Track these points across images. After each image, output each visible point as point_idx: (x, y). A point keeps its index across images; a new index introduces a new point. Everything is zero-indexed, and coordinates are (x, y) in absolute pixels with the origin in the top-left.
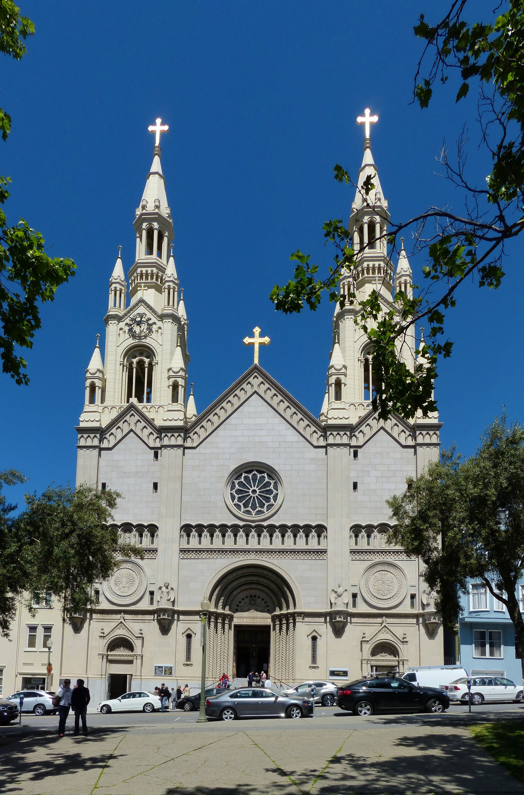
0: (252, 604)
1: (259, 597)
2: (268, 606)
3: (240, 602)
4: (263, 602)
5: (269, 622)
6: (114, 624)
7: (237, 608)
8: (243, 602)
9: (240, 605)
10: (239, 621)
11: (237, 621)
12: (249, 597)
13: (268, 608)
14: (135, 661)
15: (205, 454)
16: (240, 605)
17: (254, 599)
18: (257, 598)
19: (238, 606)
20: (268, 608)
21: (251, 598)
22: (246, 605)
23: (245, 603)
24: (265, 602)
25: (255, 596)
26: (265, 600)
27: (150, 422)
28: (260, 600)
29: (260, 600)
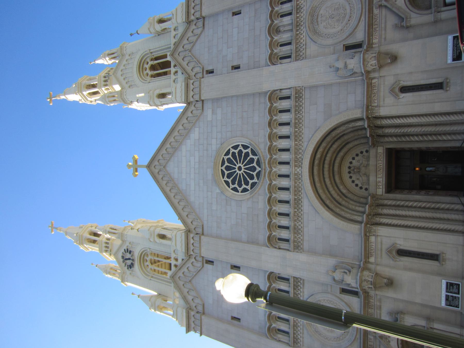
0: (359, 172)
1: (351, 163)
2: (362, 153)
3: (357, 185)
4: (357, 158)
5: (381, 150)
7: (364, 188)
8: (357, 182)
9: (360, 185)
10: (381, 187)
11: (381, 190)
12: (351, 175)
13: (364, 152)
15: (208, 215)
16: (360, 185)
18: (351, 165)
19: (361, 188)
20: (364, 152)
21: (352, 172)
22: (361, 178)
23: (358, 179)
24: (357, 155)
25: (349, 168)
26: (354, 156)
27: (185, 262)
28: (354, 162)
29: (354, 162)
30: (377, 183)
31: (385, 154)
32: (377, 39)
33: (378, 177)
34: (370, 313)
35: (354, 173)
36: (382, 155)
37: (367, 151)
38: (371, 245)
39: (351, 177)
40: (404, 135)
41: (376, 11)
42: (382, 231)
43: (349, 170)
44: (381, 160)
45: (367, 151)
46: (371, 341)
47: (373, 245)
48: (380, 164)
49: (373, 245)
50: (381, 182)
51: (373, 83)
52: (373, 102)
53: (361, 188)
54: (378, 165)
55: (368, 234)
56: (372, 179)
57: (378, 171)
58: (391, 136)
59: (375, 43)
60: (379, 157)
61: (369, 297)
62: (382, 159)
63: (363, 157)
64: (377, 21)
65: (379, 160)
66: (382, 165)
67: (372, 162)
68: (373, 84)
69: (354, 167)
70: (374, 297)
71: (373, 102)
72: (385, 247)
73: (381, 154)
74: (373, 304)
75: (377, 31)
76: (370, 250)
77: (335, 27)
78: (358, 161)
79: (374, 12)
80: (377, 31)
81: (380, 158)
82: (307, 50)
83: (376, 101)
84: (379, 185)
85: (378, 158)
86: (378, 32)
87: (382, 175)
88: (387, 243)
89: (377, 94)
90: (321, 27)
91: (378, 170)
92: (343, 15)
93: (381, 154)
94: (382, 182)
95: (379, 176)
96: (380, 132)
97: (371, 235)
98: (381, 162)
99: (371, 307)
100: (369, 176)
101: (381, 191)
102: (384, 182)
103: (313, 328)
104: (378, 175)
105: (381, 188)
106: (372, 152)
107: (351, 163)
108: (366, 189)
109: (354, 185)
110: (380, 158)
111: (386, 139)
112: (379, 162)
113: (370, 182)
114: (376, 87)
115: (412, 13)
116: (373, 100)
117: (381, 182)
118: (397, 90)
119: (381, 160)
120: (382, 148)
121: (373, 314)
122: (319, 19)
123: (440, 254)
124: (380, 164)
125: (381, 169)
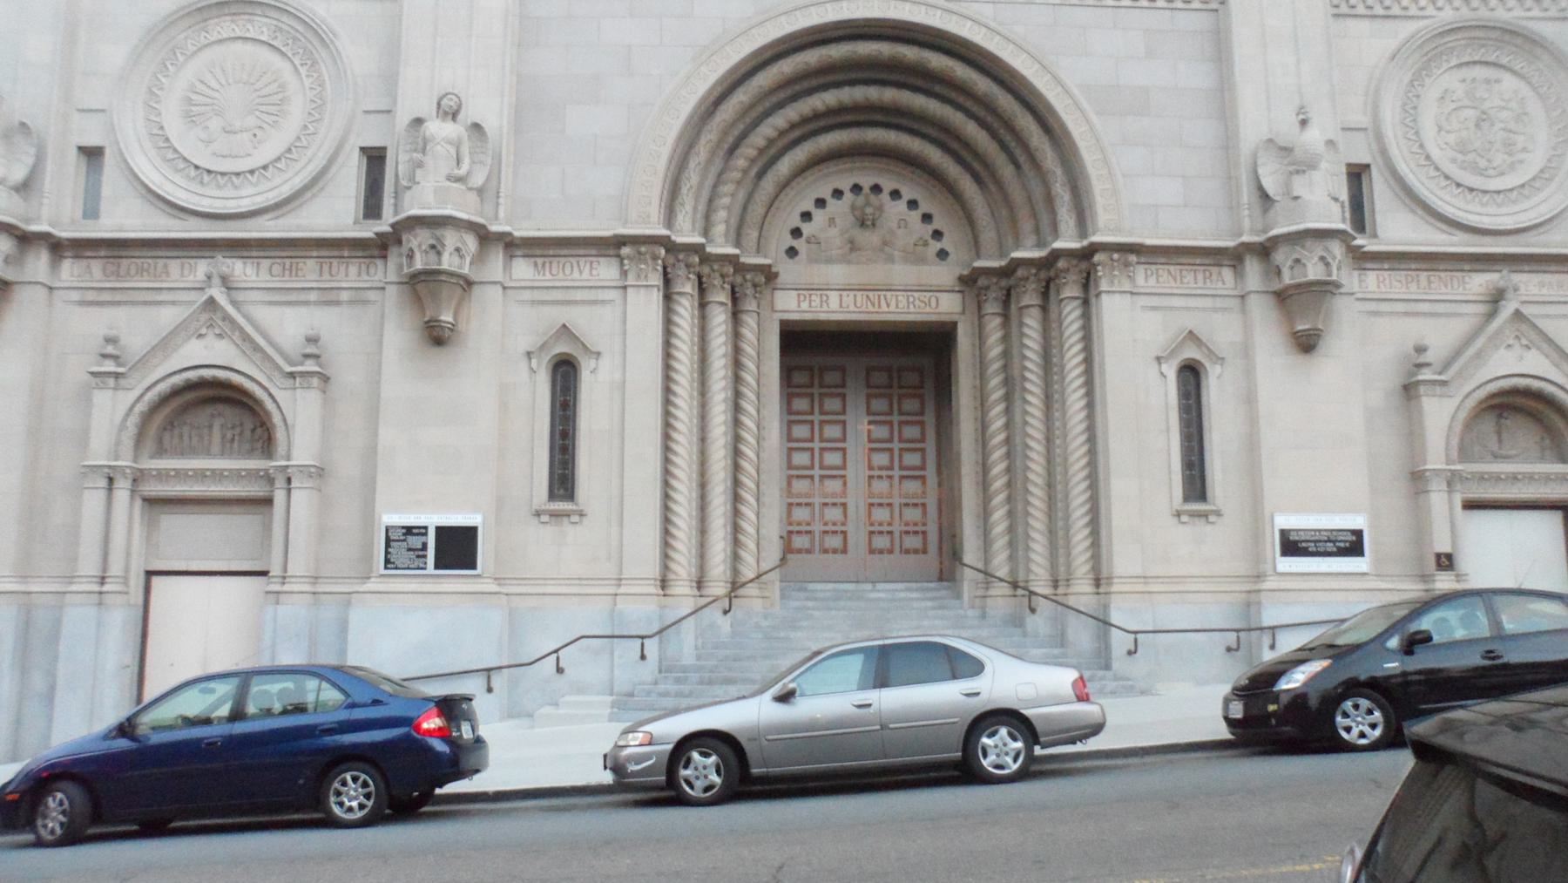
1: (895, 194)
2: (937, 235)
5: (947, 306)
6: (168, 317)
7: (796, 243)
8: (819, 216)
9: (807, 229)
10: (805, 306)
12: (848, 196)
14: (279, 497)
16: (807, 229)
17: (873, 198)
18: (885, 196)
19: (796, 233)
21: (860, 200)
22: (834, 232)
23: (832, 221)
24: (927, 218)
28: (901, 206)
29: (901, 206)
30: (819, 292)
31: (934, 318)
32: (1379, 287)
33: (845, 293)
34: (301, 265)
36: (928, 309)
38: (582, 264)
39: (838, 193)
41: (1480, 282)
42: (645, 305)
43: (866, 189)
44: (911, 306)
45: (942, 254)
46: (186, 272)
47: (581, 272)
48: (893, 303)
49: (581, 272)
50: (825, 304)
51: (1220, 273)
52: (1149, 272)
54: (889, 294)
55: (626, 251)
56: (837, 273)
57: (867, 296)
59: (1363, 277)
60: (922, 298)
61: (367, 261)
62: (912, 309)
63: (921, 243)
64: (1443, 287)
65: (911, 299)
66: (892, 308)
67: (902, 273)
68: (1215, 270)
69: (880, 208)
70: (368, 278)
71: (1149, 272)
72: (579, 319)
73: (933, 304)
74: (338, 278)
75: (1408, 288)
76: (563, 260)
77: (1443, 133)
78: (903, 223)
79: (1474, 275)
80: (1408, 288)
81: (917, 302)
82: (1365, 25)
83: (1152, 281)
84: (813, 297)
85: (916, 294)
86: (1404, 290)
87: (852, 308)
88: (595, 325)
89: (1178, 284)
90: (1448, 80)
91: (871, 294)
92: (1483, 163)
93: (933, 304)
94: (825, 308)
95: (848, 298)
97: (626, 262)
98: (901, 305)
99: (326, 268)
100: (849, 262)
101: (792, 305)
102: (823, 317)
103: (186, 38)
104: (852, 294)
105: (799, 306)
108: (792, 252)
109: (808, 205)
110: (917, 302)
112: (900, 298)
113: (823, 266)
114: (1205, 283)
115: (1456, 401)
116: (1157, 270)
117: (825, 304)
118: (1191, 353)
119: (911, 306)
120: (958, 309)
121: (297, 275)
122: (1480, 72)
123: (577, 504)
124: (893, 303)
125: (873, 305)
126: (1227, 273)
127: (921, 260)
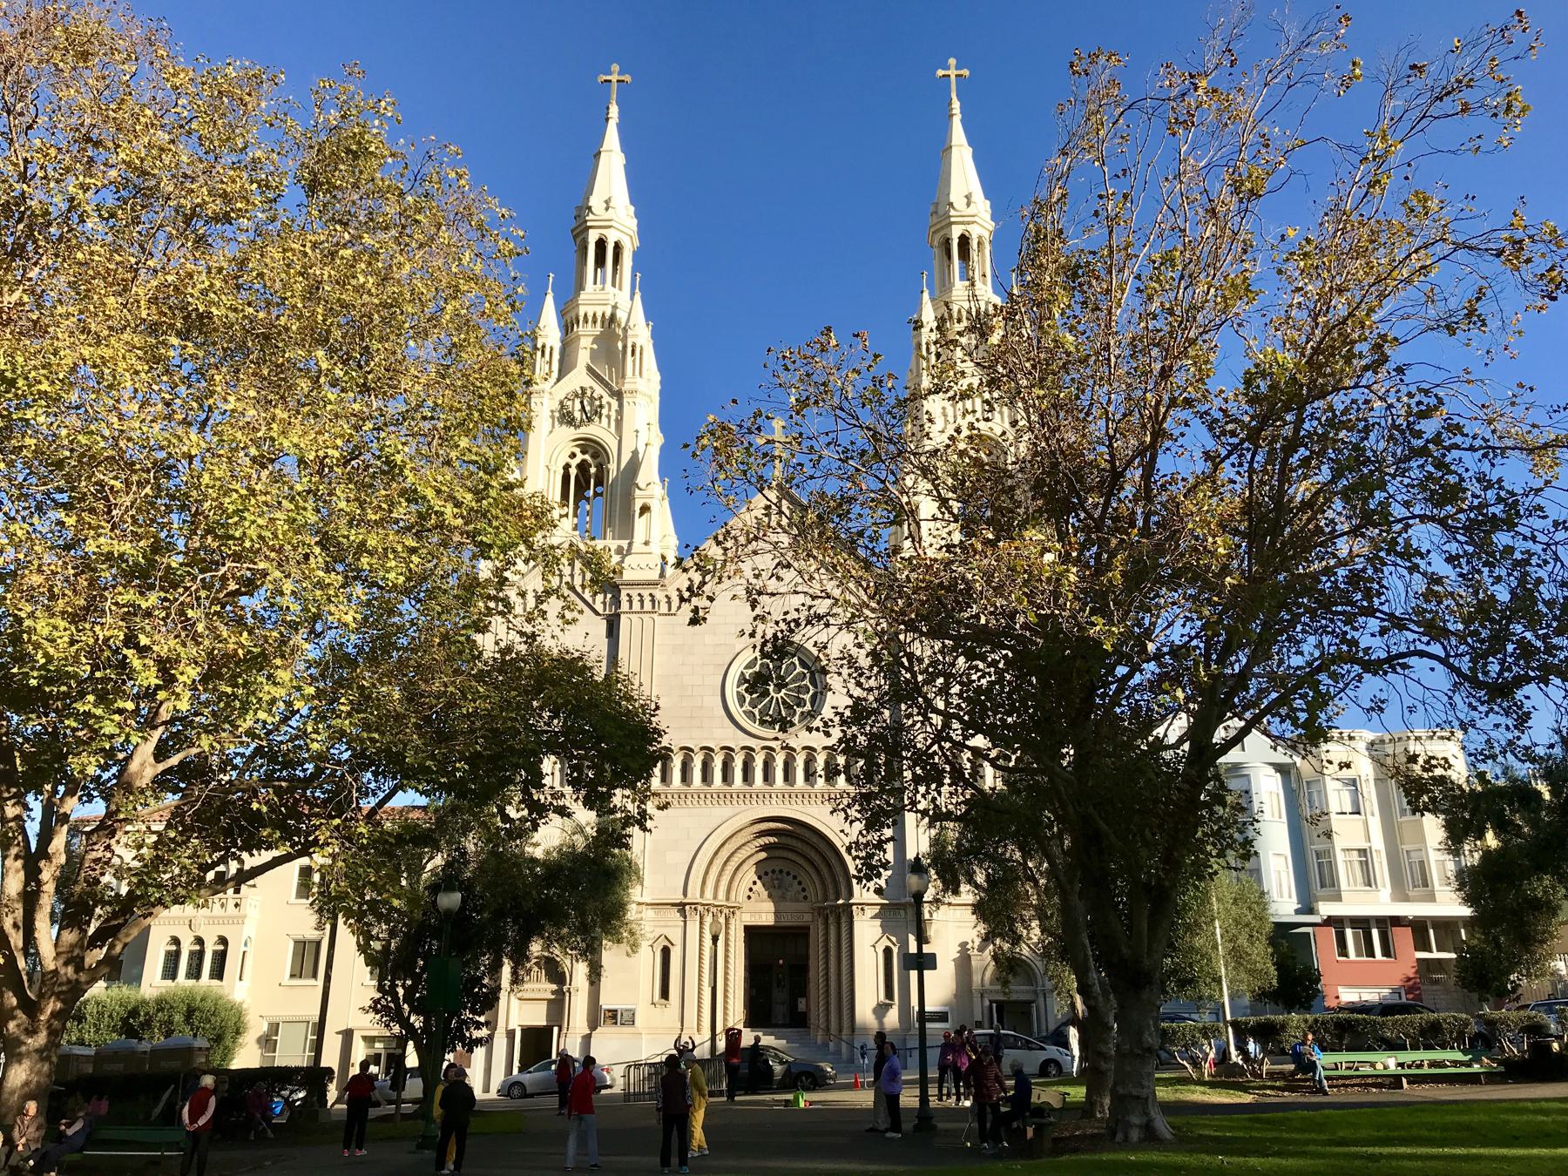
1: (788, 874)
2: (804, 890)
4: (796, 882)
5: (807, 918)
9: (754, 888)
24: (800, 883)
35: (772, 879)
37: (805, 898)
40: (827, 951)
53: (751, 890)
58: (827, 934)
96: (831, 920)
106: (804, 906)
107: (788, 874)
108: (749, 897)
111: (821, 927)
126: (902, 912)
127: (797, 901)
